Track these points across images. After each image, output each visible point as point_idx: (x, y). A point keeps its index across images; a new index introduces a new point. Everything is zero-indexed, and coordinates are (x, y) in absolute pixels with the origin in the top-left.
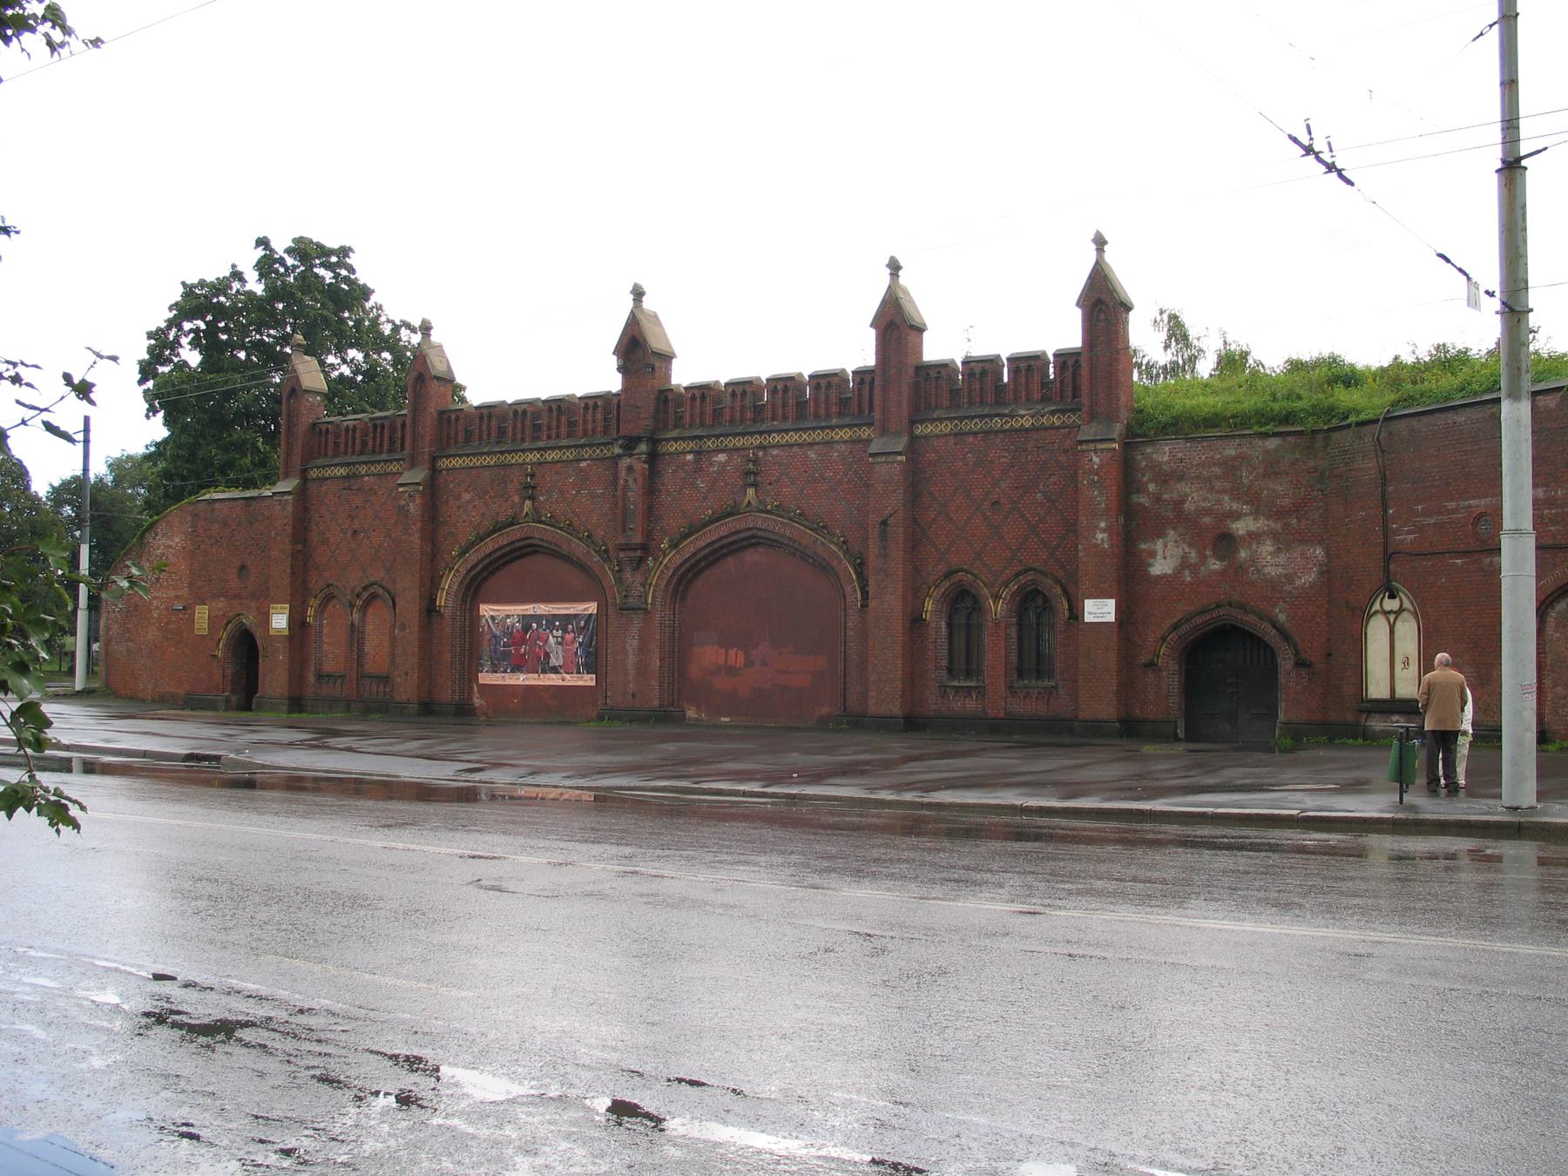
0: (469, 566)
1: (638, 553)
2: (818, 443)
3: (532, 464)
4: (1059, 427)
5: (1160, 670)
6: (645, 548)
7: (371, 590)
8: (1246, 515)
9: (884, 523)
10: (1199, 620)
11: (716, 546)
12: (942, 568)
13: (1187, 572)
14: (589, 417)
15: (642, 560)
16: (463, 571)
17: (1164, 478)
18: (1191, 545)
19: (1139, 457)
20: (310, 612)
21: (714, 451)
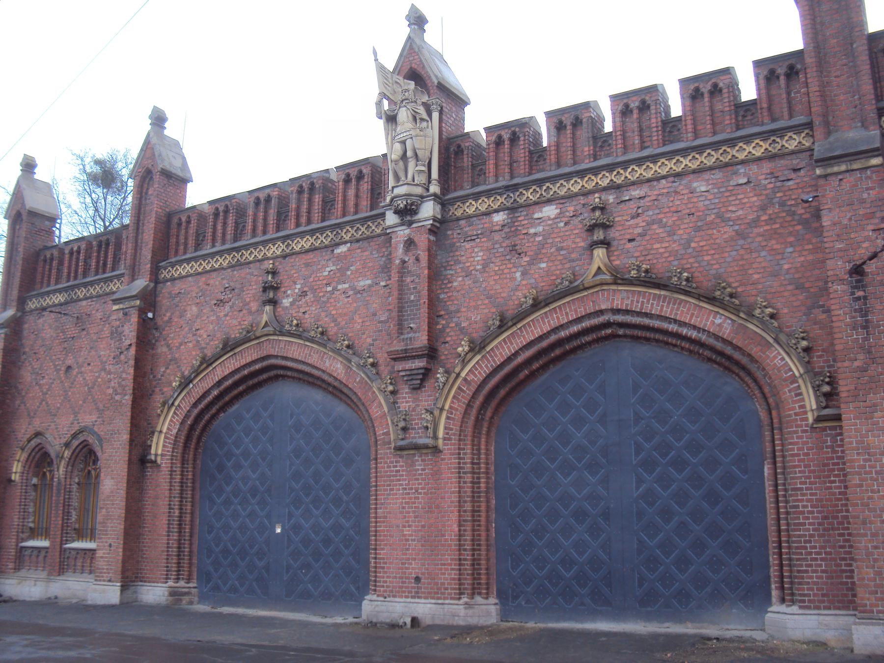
0: (193, 400)
2: (711, 168)
6: (431, 353)
7: (81, 438)
9: (858, 271)
11: (544, 344)
14: (351, 192)
15: (427, 373)
16: (186, 407)
21: (536, 203)
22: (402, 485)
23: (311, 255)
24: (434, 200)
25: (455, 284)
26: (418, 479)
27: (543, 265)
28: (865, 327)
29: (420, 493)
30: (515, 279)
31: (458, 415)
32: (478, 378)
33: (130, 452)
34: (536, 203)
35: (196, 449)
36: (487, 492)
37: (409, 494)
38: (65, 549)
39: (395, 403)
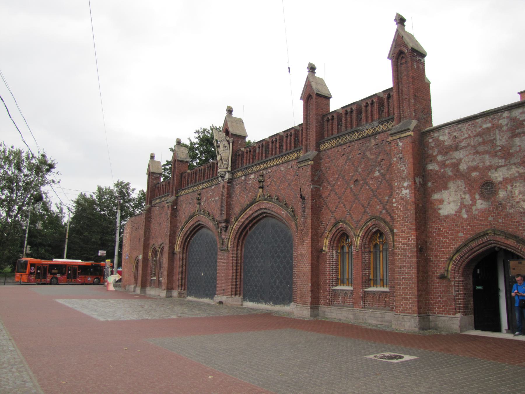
0: (184, 234)
1: (224, 224)
2: (284, 163)
3: (200, 190)
4: (385, 131)
5: (449, 280)
8: (501, 166)
10: (473, 244)
12: (333, 221)
13: (464, 211)
15: (227, 227)
17: (446, 150)
18: (465, 193)
19: (430, 141)
20: (150, 254)
21: (250, 174)
23: (207, 189)
24: (228, 173)
25: (234, 199)
27: (251, 194)
28: (304, 217)
30: (245, 198)
31: (233, 240)
32: (237, 229)
33: (169, 251)
34: (250, 174)
35: (187, 249)
36: (241, 264)
38: (160, 280)
39: (221, 236)
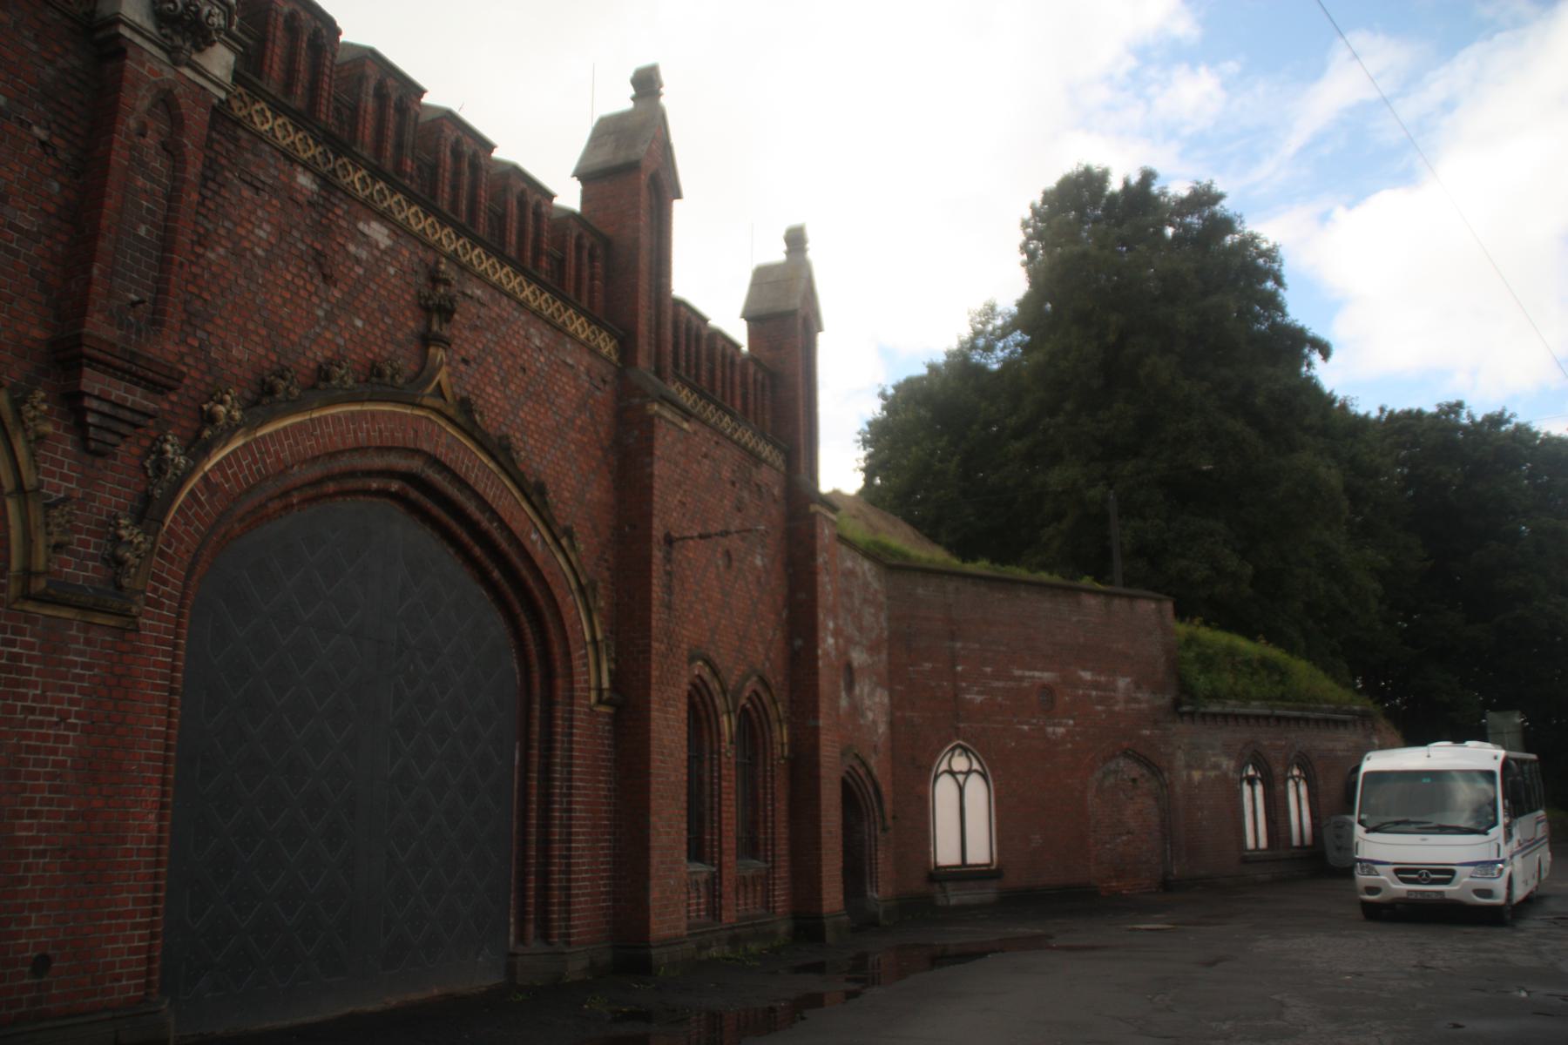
22: (24, 697)
26: (70, 689)
29: (73, 727)
37: (40, 724)
